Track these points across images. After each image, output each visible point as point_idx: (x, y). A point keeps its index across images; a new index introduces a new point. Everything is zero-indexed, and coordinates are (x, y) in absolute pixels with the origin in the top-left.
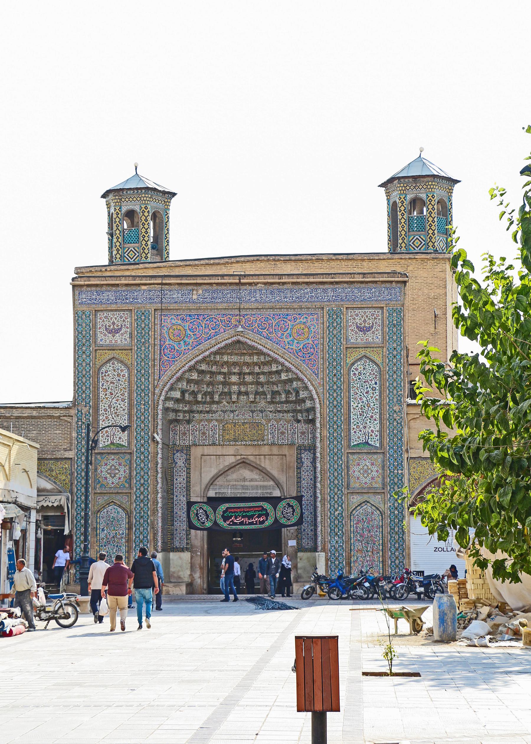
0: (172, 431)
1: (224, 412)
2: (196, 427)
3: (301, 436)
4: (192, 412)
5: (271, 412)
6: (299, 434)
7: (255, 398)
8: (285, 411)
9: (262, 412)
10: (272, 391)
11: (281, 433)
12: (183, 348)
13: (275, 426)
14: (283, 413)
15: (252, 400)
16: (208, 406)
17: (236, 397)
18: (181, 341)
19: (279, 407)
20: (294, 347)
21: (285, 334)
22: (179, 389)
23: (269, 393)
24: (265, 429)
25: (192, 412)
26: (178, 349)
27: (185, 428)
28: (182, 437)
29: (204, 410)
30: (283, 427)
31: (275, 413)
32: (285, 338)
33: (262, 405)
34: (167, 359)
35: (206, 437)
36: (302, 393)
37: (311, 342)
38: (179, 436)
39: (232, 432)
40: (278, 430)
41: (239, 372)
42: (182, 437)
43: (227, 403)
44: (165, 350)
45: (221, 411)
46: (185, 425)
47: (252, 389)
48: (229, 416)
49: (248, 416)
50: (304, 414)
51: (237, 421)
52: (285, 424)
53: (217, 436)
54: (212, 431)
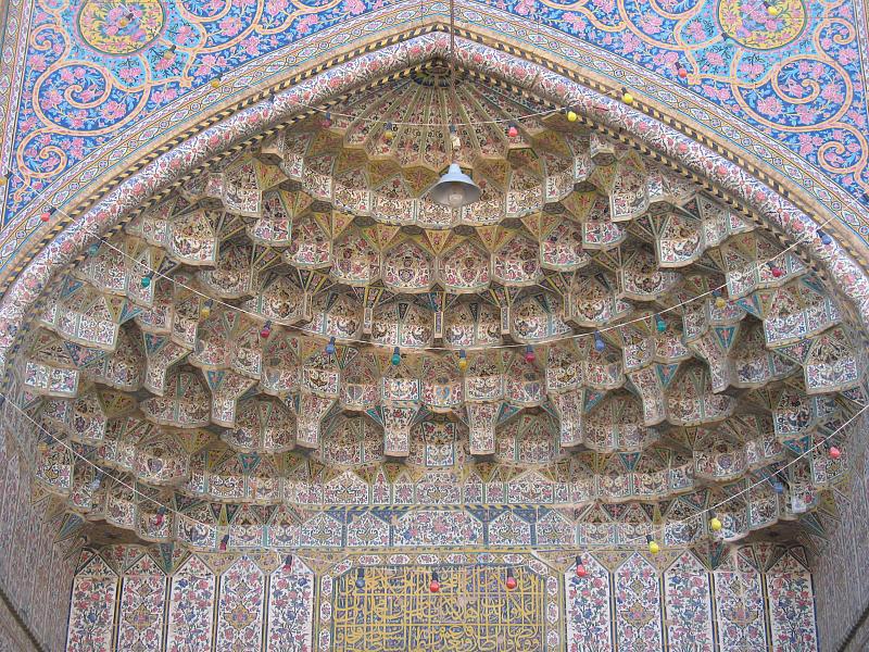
0: (82, 607)
1: (346, 515)
2: (202, 585)
3: (731, 631)
4: (187, 504)
5: (577, 513)
6: (721, 621)
7: (497, 448)
8: (647, 507)
9: (528, 514)
10: (589, 392)
11: (630, 614)
12: (147, 83)
13: (597, 584)
14: (635, 522)
15: (481, 451)
16: (269, 483)
17: (403, 435)
18: (138, 50)
19: (617, 489)
20: (733, 78)
21: (683, 20)
22: (114, 300)
23: (570, 406)
24: (546, 599)
25: (187, 504)
26: (118, 85)
27: (145, 590)
28: (130, 634)
29: (248, 498)
30: (637, 586)
31: (597, 521)
32: (679, 39)
33: (530, 487)
34: (56, 129)
35: (250, 633)
36: (779, 322)
37: (820, 56)
38: (115, 632)
39: (381, 610)
40: (614, 601)
41: (425, 288)
42: (130, 634)
43: (361, 473)
44: (52, 92)
45: (332, 511)
46: (146, 577)
47: (486, 396)
48: (367, 536)
49: (460, 538)
50: (753, 508)
51: (407, 560)
52: (645, 574)
53: (308, 627)
54: (280, 605)
